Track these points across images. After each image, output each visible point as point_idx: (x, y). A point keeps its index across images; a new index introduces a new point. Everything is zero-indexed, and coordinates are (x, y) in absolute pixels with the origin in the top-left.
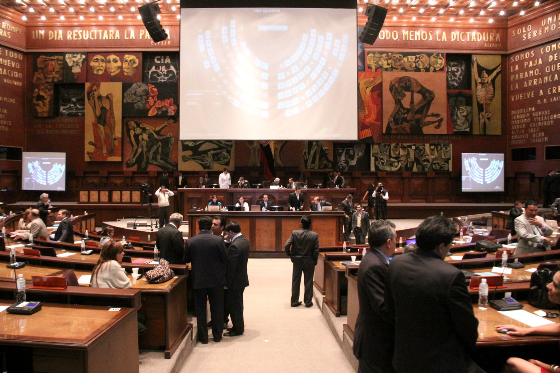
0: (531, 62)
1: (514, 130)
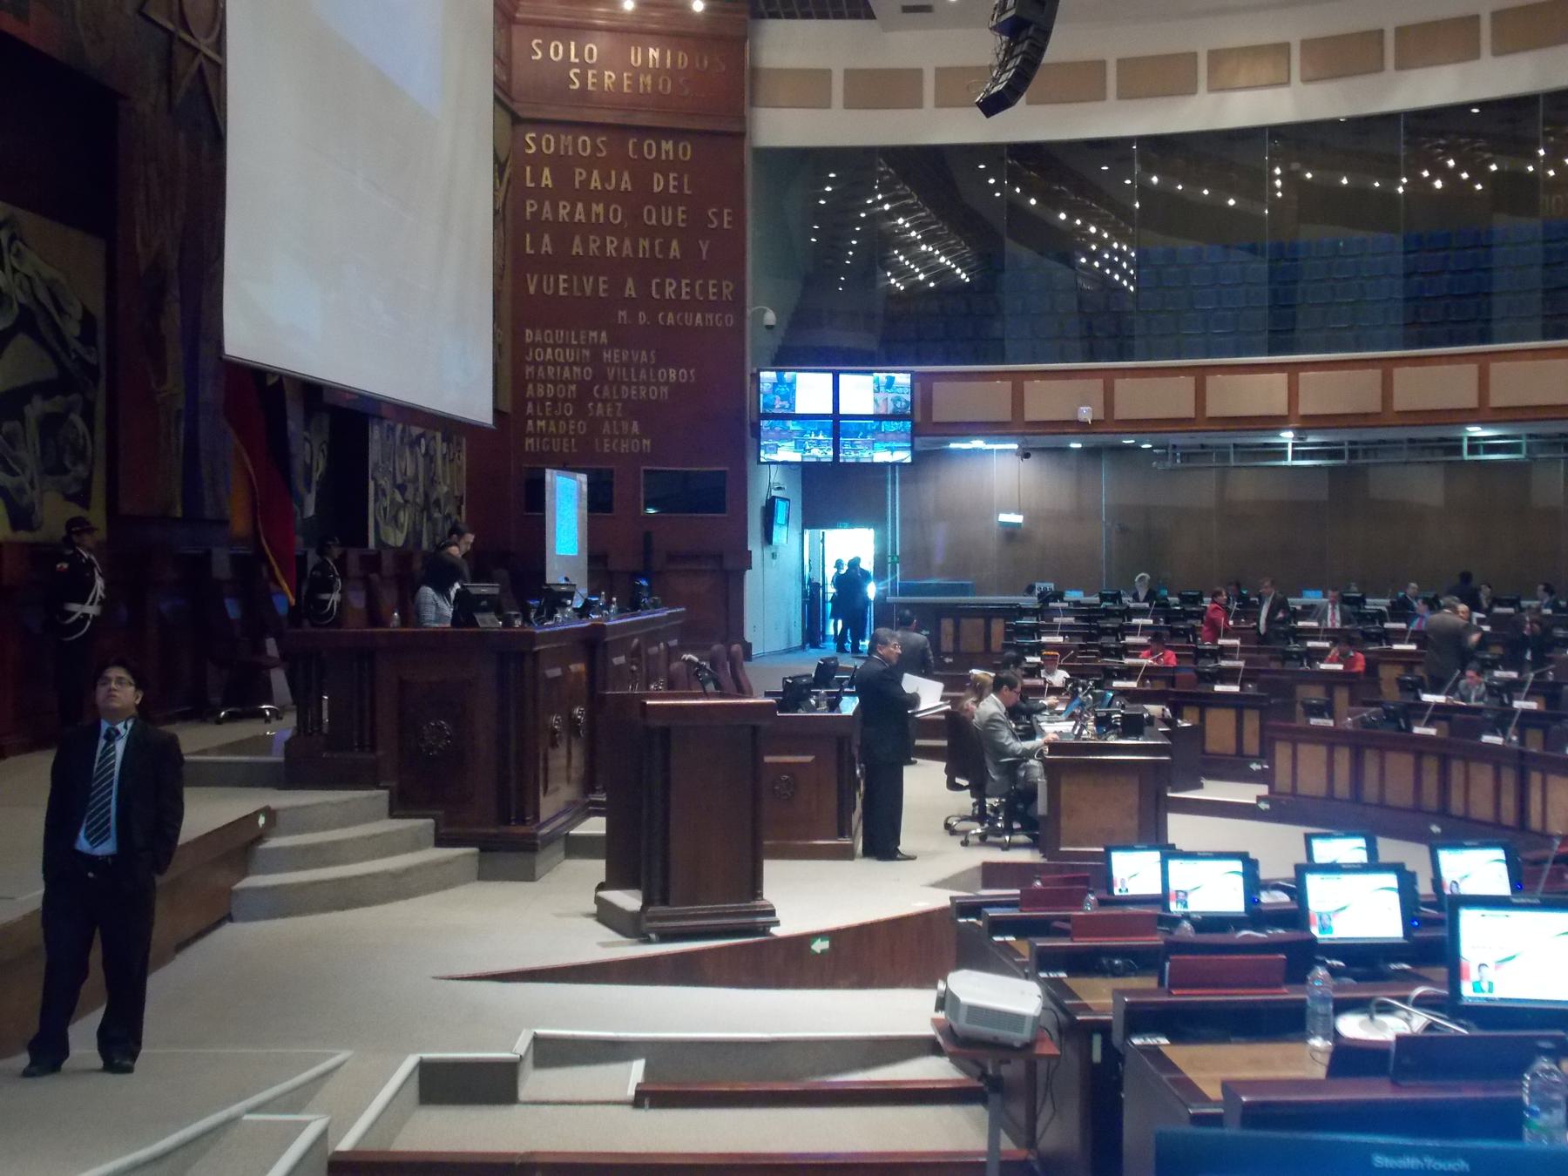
0: (595, 174)
1: (535, 400)
